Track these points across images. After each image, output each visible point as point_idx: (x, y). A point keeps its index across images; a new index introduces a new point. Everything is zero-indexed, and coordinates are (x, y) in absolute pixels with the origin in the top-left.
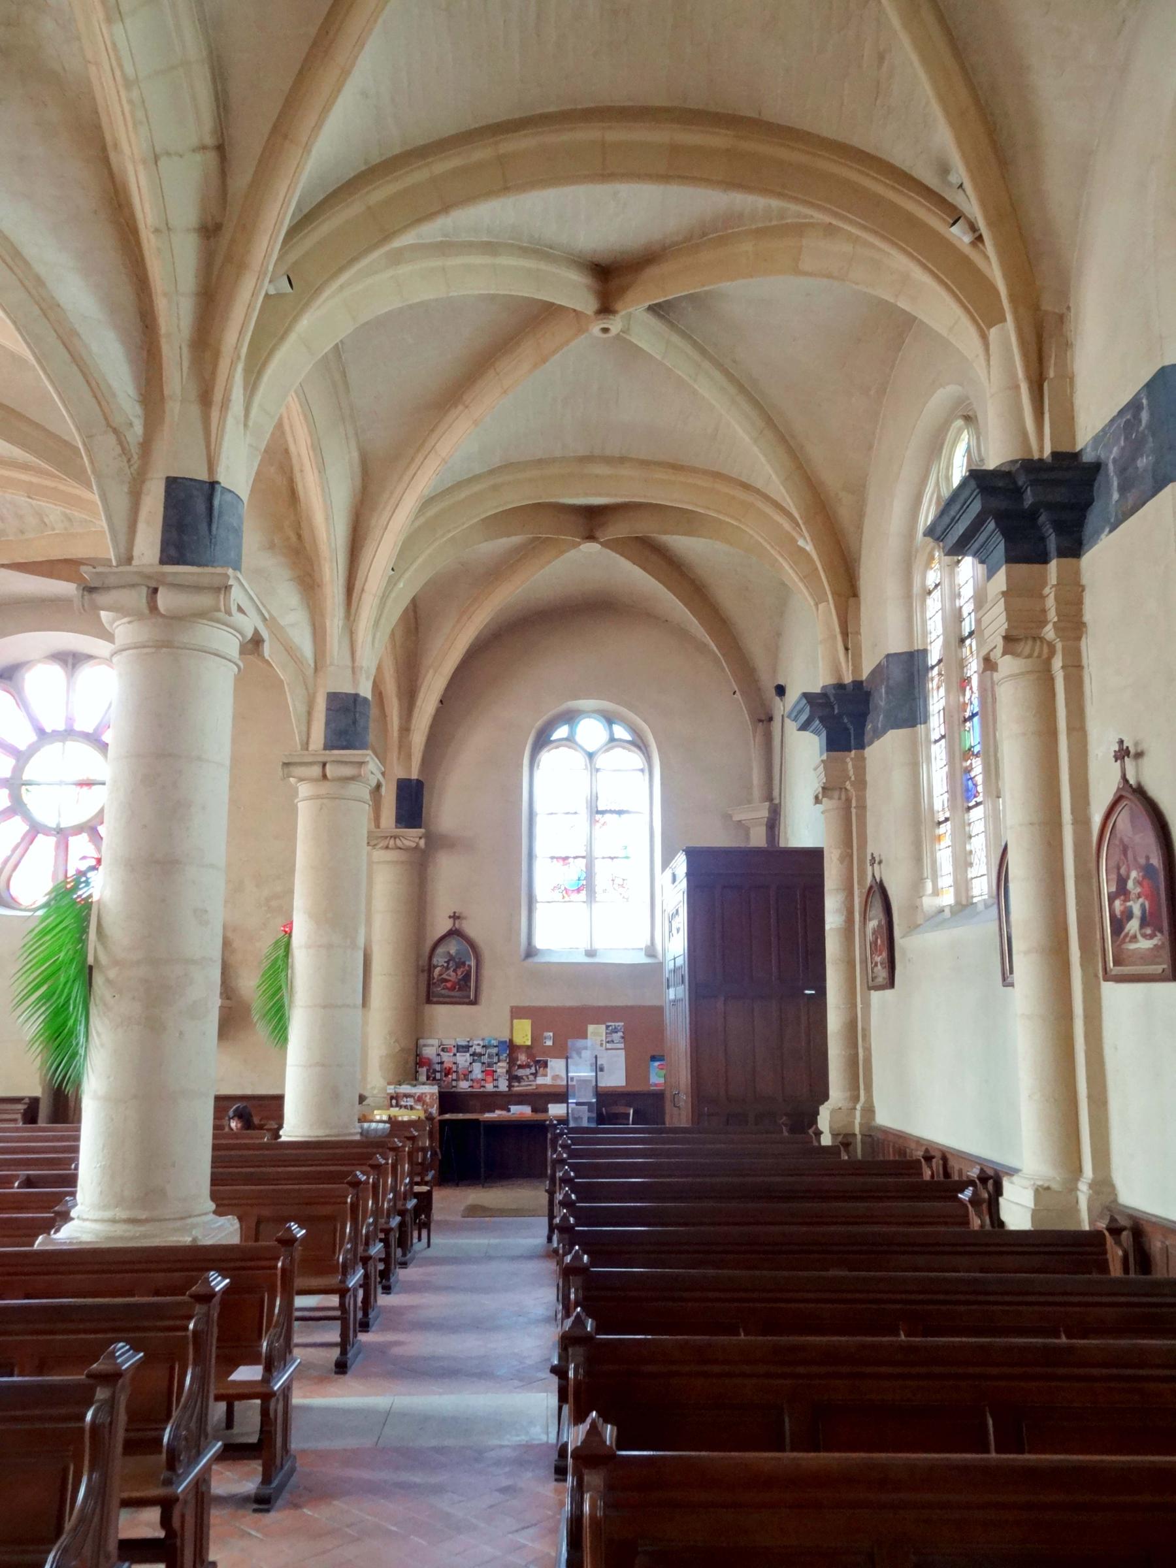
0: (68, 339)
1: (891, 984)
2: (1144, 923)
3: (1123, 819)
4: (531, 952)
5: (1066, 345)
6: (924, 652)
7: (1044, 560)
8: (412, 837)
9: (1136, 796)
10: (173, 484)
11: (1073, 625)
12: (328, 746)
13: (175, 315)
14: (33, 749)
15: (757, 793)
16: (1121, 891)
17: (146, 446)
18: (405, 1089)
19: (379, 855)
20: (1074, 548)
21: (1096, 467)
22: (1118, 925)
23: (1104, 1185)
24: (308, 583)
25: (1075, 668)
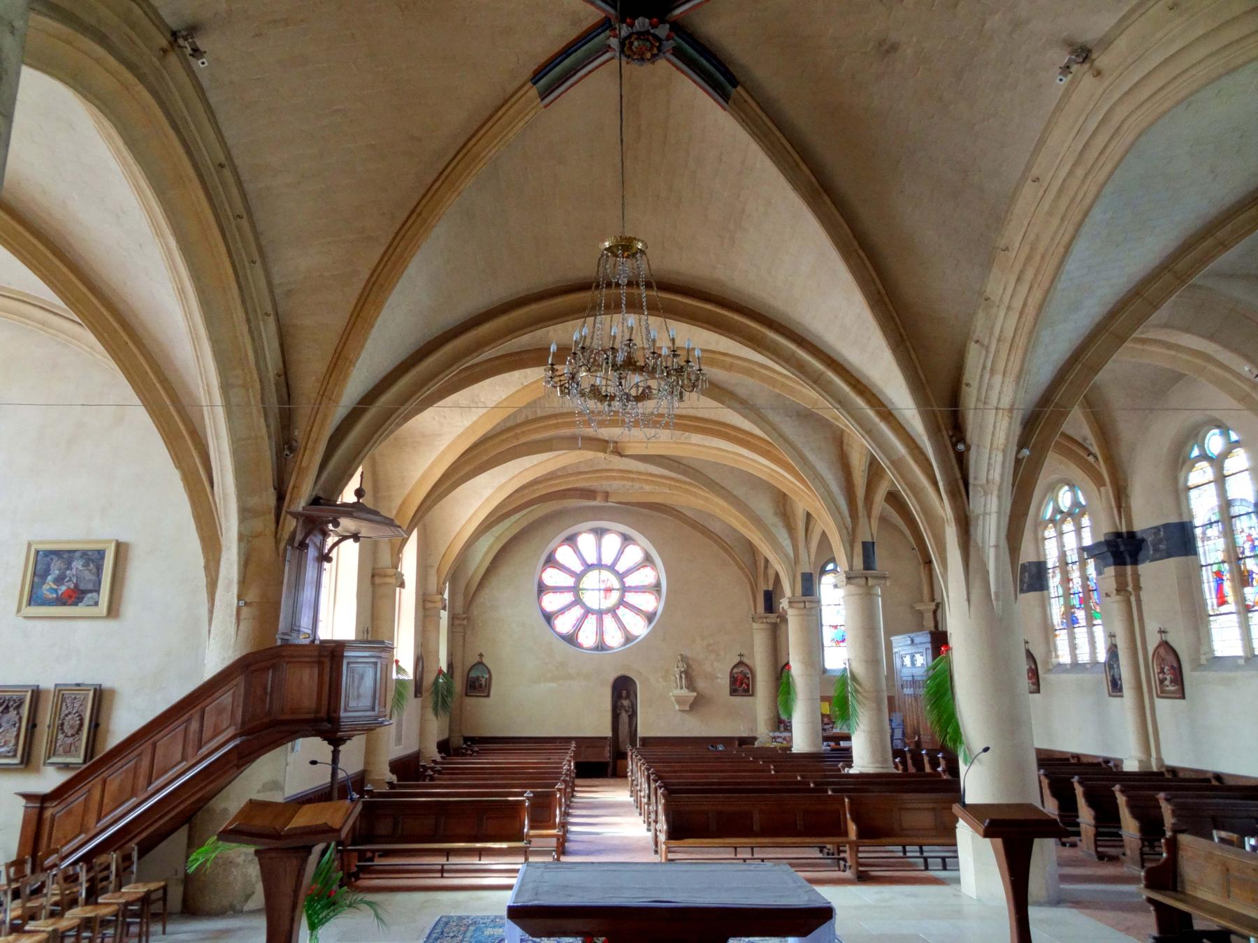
0: (834, 501)
1: (1038, 691)
2: (1172, 681)
3: (1162, 651)
4: (825, 671)
5: (1128, 497)
6: (1045, 563)
7: (1125, 564)
8: (772, 618)
9: (1165, 644)
10: (864, 543)
11: (1138, 588)
12: (804, 595)
13: (860, 492)
14: (583, 573)
15: (926, 596)
16: (1162, 671)
17: (854, 530)
18: (777, 734)
19: (755, 626)
20: (1135, 562)
21: (1143, 540)
22: (1162, 681)
23: (1159, 759)
24: (790, 529)
25: (1139, 601)
